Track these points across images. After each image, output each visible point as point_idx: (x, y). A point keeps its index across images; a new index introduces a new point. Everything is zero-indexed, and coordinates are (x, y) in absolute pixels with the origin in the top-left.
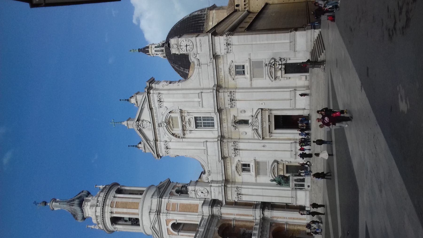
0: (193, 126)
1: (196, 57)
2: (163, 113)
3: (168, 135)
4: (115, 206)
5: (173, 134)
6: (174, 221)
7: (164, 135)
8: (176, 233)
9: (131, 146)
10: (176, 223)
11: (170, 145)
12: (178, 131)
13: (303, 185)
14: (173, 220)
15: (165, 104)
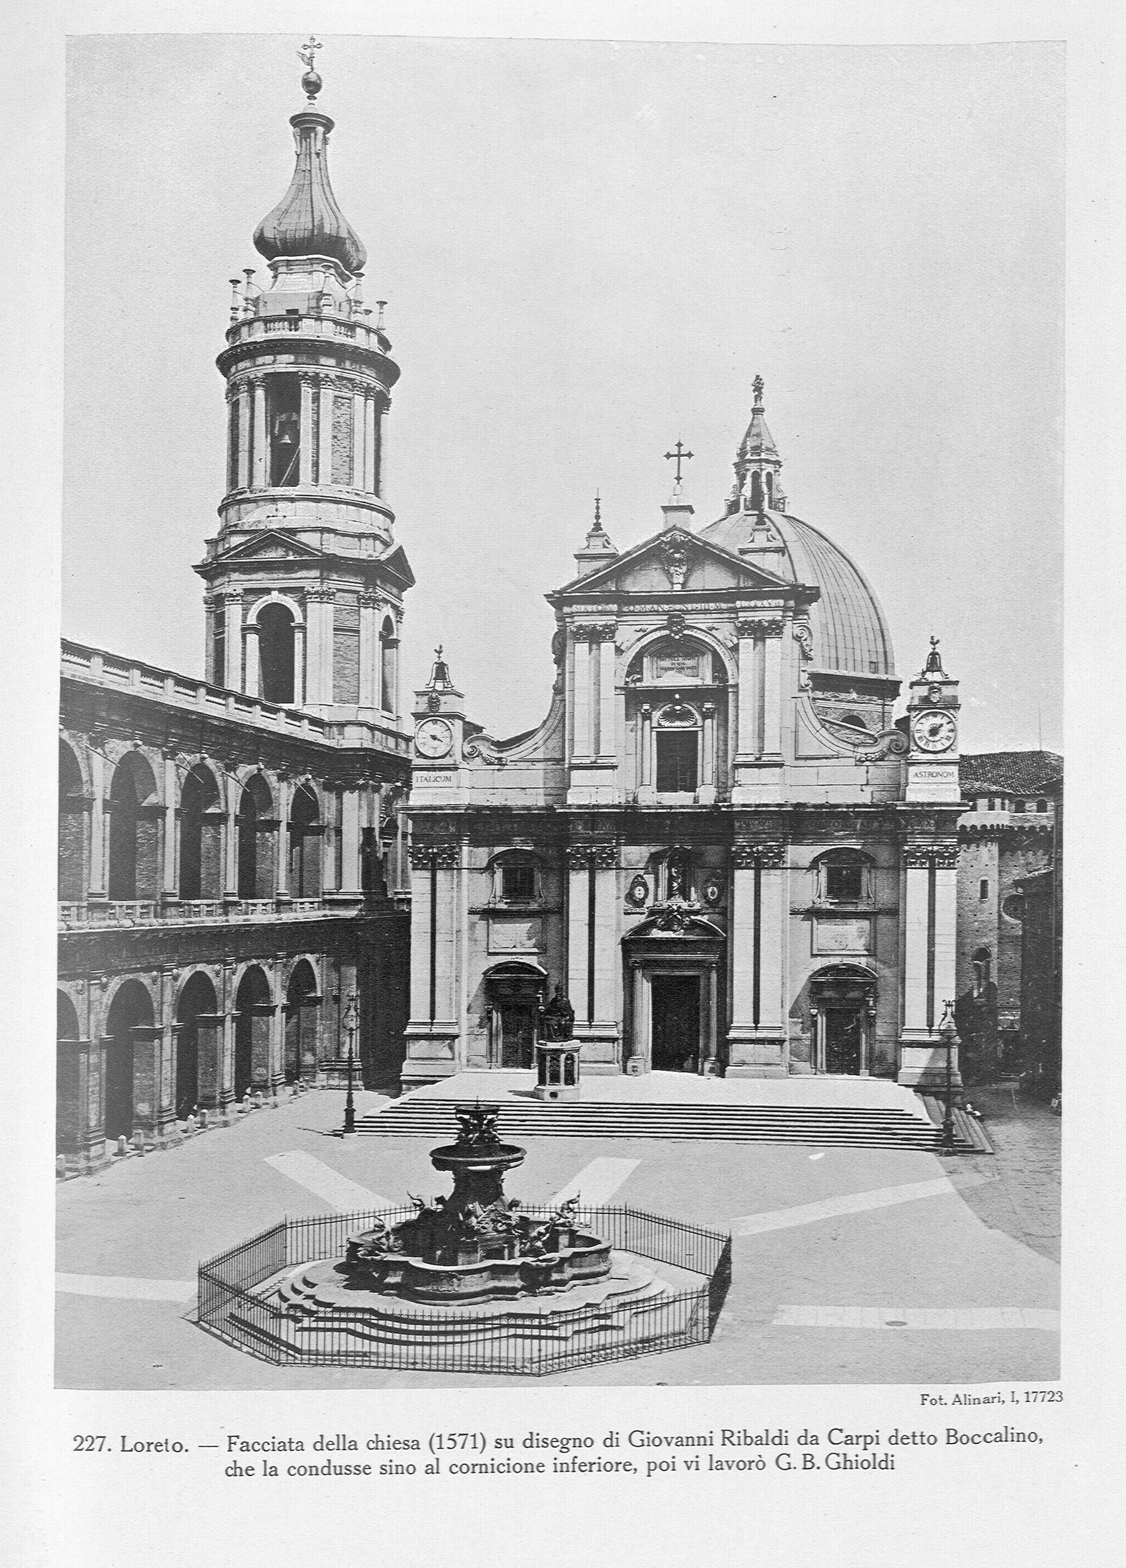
0: (663, 723)
1: (892, 752)
2: (714, 632)
3: (639, 640)
4: (337, 393)
5: (638, 658)
6: (298, 619)
7: (638, 627)
8: (252, 620)
9: (598, 508)
10: (293, 624)
11: (607, 648)
12: (654, 677)
13: (555, 1079)
14: (305, 618)
15: (746, 643)
